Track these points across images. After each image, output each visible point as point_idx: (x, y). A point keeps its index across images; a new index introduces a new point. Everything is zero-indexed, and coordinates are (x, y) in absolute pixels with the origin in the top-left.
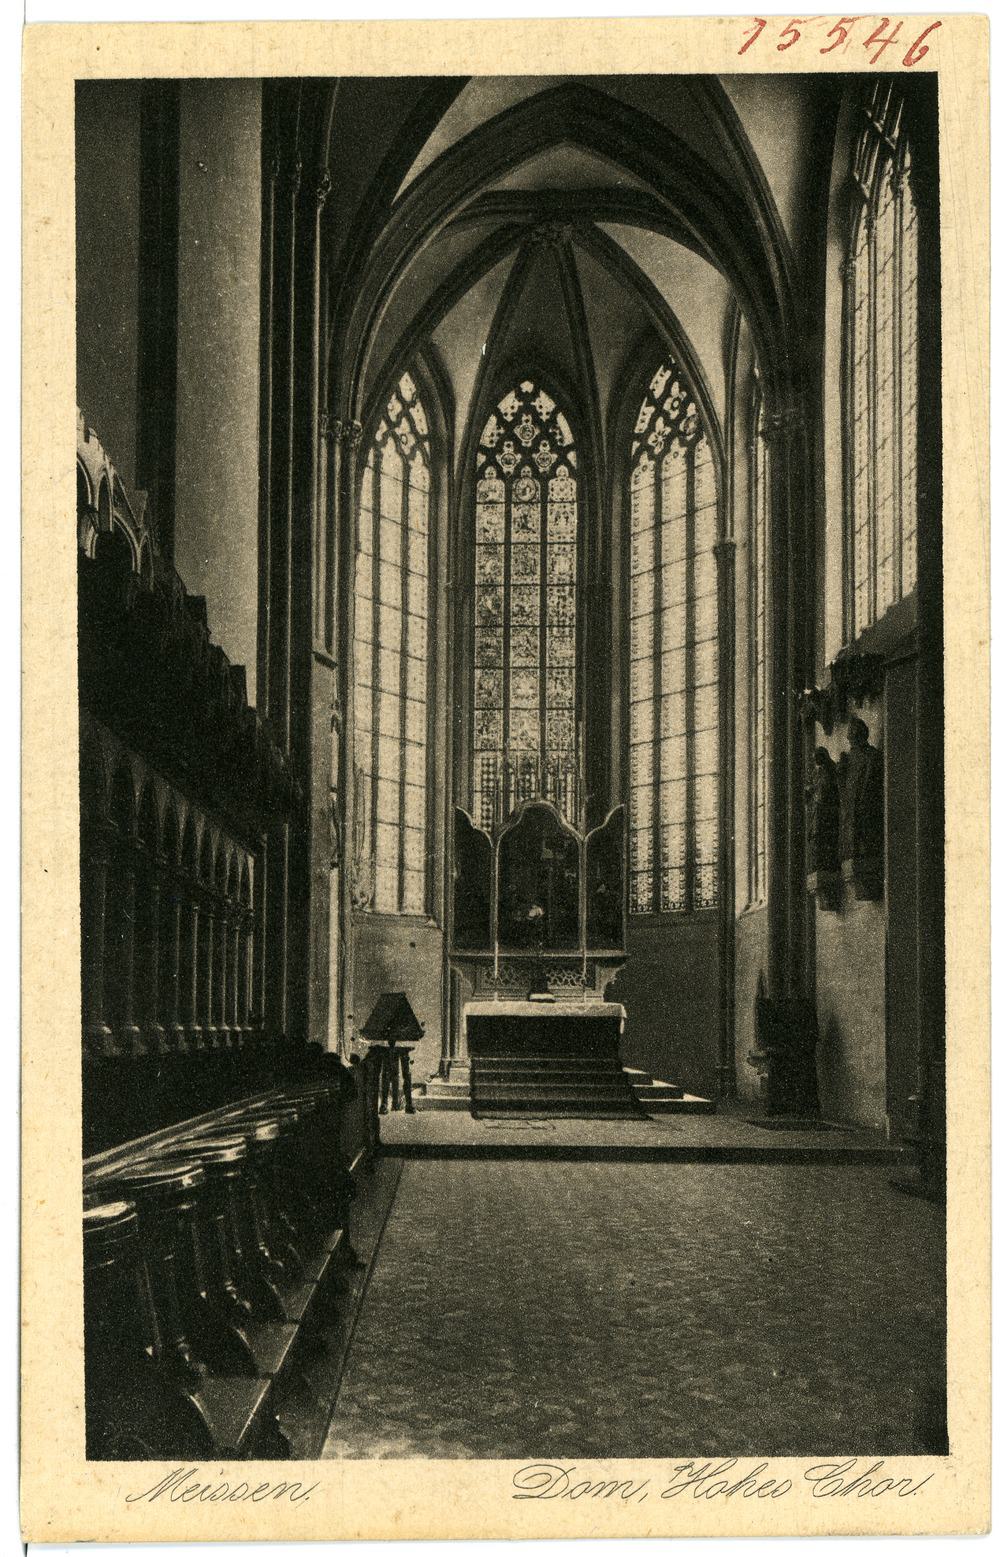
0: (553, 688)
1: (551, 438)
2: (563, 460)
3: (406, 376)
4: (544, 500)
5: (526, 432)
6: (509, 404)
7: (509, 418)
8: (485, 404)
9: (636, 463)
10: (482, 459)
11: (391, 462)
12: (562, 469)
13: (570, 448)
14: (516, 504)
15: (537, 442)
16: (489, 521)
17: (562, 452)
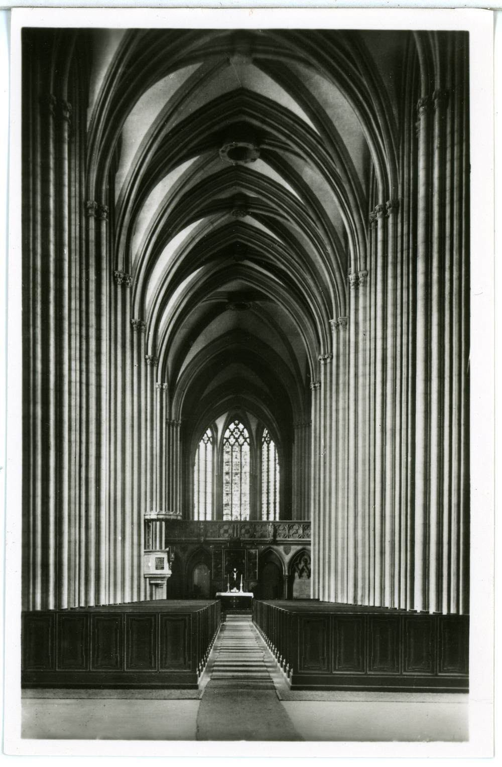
0: (243, 499)
1: (243, 435)
3: (209, 430)
4: (241, 451)
6: (232, 426)
7: (232, 430)
8: (226, 427)
9: (263, 443)
10: (225, 440)
11: (202, 444)
12: (245, 443)
13: (247, 438)
14: (234, 452)
15: (239, 436)
16: (226, 457)
17: (245, 439)
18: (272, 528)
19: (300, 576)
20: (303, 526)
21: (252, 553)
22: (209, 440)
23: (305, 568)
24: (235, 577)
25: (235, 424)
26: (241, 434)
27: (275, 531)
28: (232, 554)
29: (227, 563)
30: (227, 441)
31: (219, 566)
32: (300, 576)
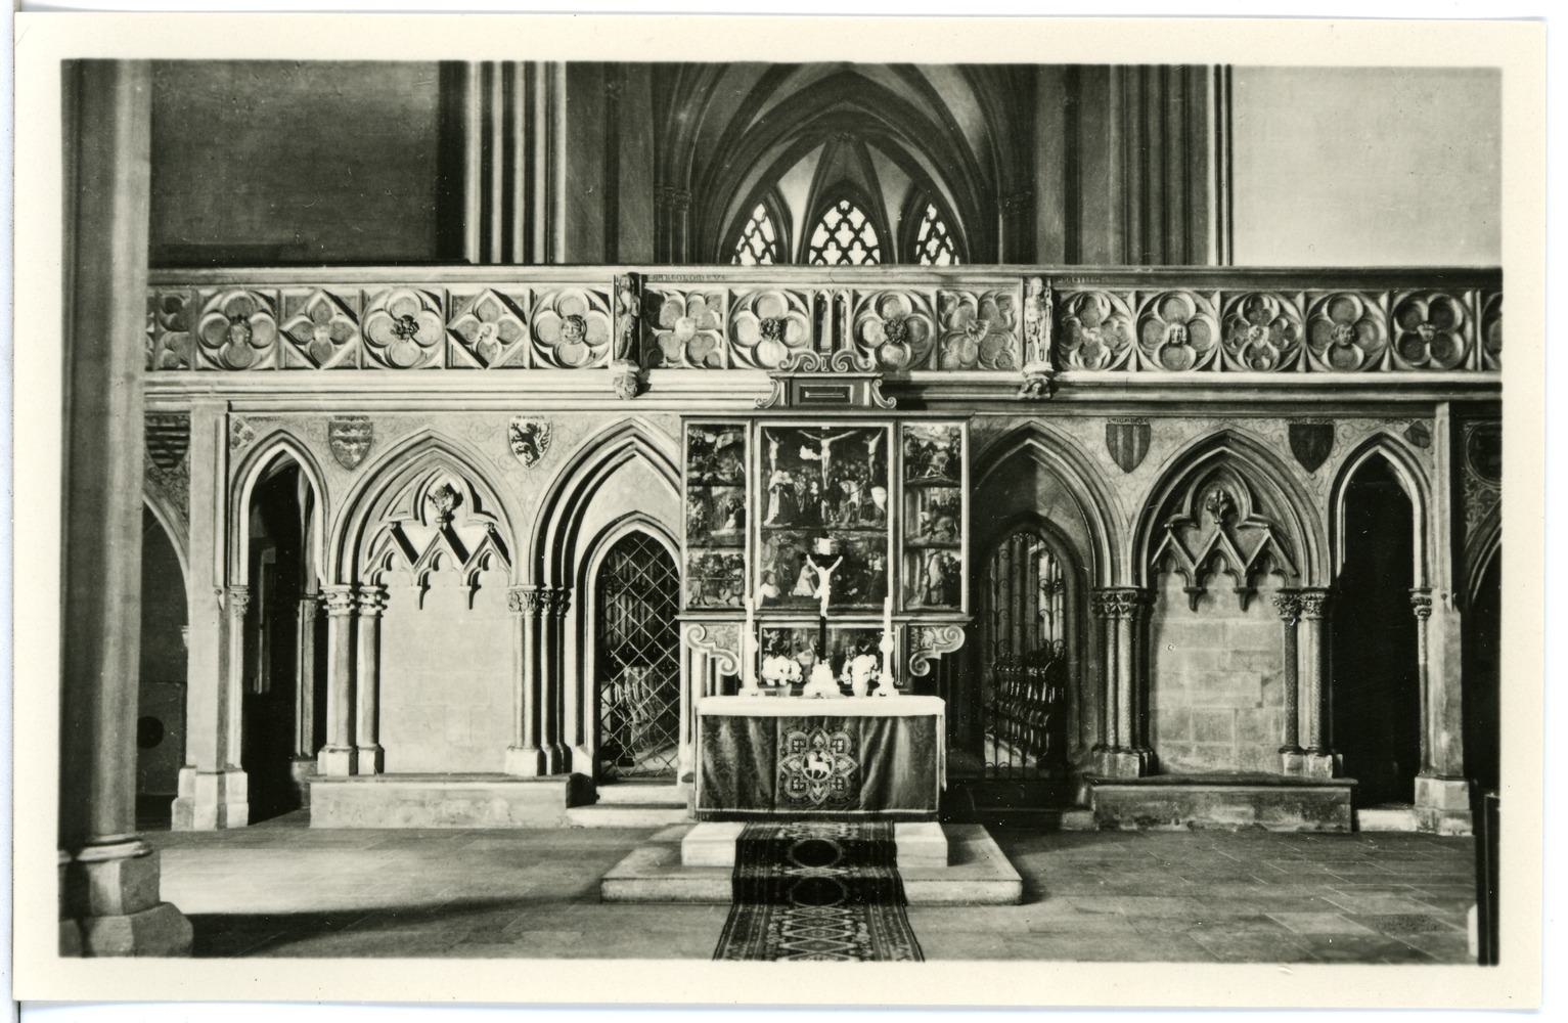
2: (870, 256)
5: (844, 236)
6: (832, 217)
7: (832, 226)
8: (815, 218)
10: (813, 255)
15: (852, 243)
17: (869, 251)
18: (1042, 305)
19: (1198, 595)
20: (1224, 298)
21: (931, 446)
22: (767, 249)
23: (1226, 546)
24: (824, 592)
25: (840, 210)
26: (857, 238)
27: (1062, 334)
28: (806, 453)
29: (774, 509)
30: (820, 256)
31: (728, 528)
32: (1198, 595)
